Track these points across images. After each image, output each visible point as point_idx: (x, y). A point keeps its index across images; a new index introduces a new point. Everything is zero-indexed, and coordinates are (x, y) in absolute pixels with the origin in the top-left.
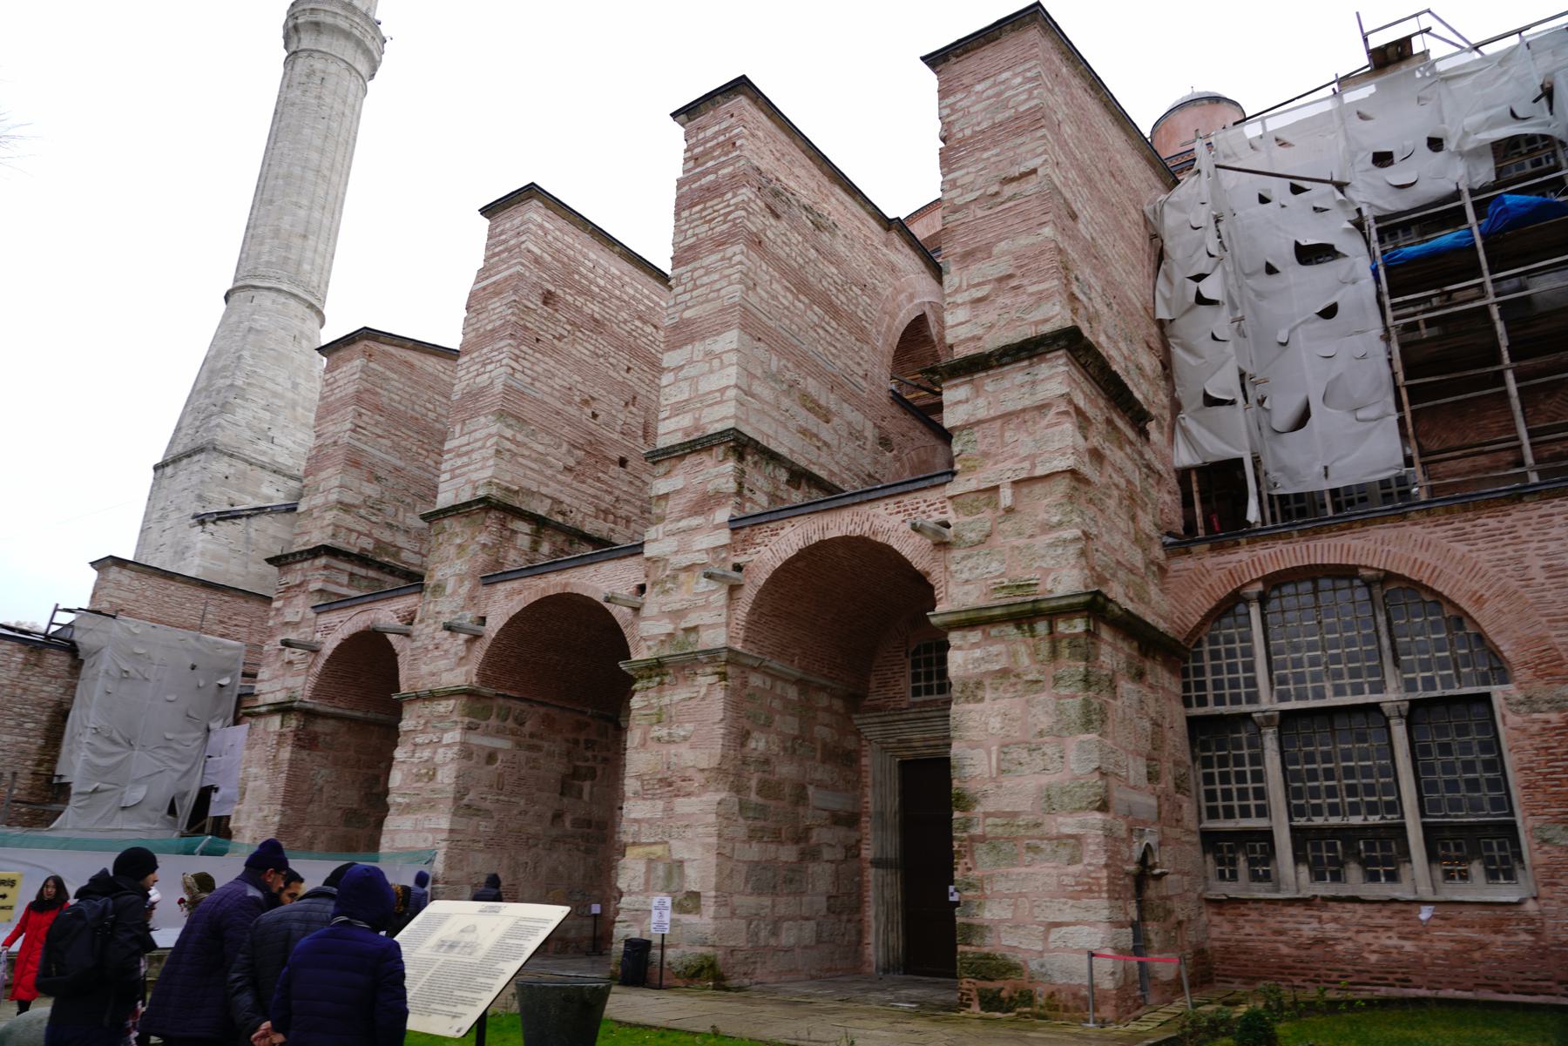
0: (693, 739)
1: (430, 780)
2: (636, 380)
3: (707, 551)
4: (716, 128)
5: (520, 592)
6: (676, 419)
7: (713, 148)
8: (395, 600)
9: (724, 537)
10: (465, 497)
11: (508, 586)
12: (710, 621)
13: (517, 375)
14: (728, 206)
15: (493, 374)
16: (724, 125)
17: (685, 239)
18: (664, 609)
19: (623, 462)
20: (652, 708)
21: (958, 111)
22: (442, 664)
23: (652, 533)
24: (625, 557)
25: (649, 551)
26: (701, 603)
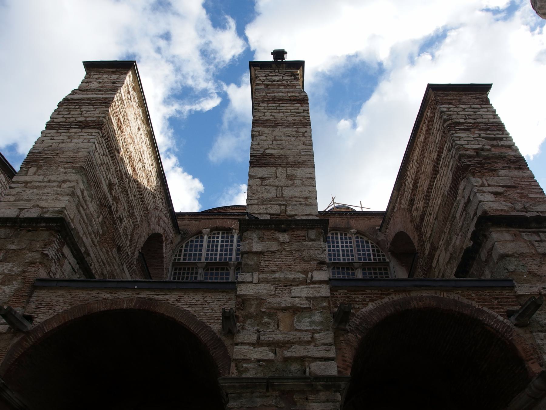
2: (135, 204)
3: (308, 298)
4: (281, 78)
6: (265, 207)
7: (279, 85)
9: (325, 291)
10: (34, 213)
12: (318, 355)
13: (97, 154)
14: (298, 109)
15: (78, 145)
16: (285, 78)
17: (264, 116)
18: (262, 338)
19: (119, 249)
21: (450, 111)
23: (246, 277)
25: (242, 290)
26: (308, 337)
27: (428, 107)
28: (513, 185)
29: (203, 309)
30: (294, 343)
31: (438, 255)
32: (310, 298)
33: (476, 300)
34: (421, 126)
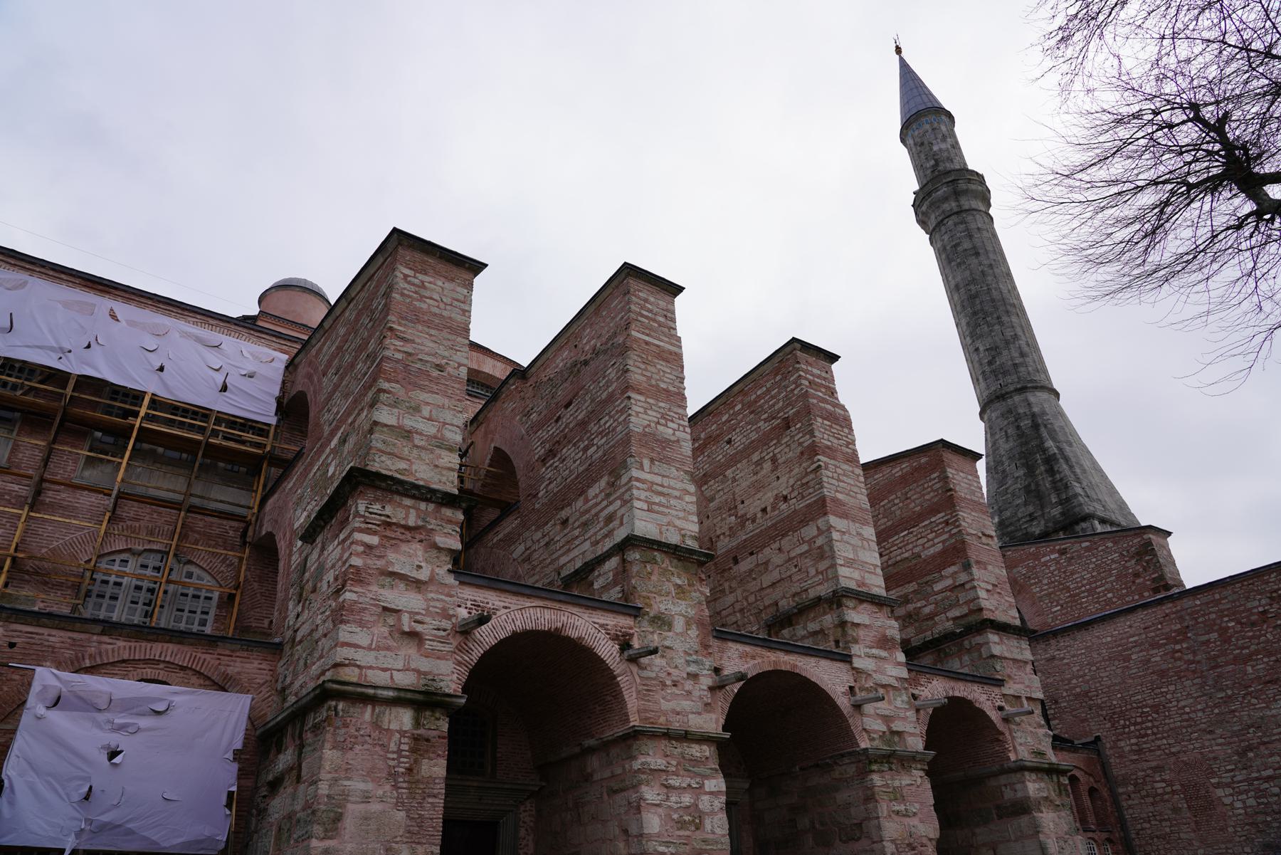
0: (920, 815)
1: (697, 829)
5: (753, 658)
8: (600, 613)
11: (741, 647)
18: (878, 711)
20: (889, 787)
22: (686, 704)
24: (836, 660)
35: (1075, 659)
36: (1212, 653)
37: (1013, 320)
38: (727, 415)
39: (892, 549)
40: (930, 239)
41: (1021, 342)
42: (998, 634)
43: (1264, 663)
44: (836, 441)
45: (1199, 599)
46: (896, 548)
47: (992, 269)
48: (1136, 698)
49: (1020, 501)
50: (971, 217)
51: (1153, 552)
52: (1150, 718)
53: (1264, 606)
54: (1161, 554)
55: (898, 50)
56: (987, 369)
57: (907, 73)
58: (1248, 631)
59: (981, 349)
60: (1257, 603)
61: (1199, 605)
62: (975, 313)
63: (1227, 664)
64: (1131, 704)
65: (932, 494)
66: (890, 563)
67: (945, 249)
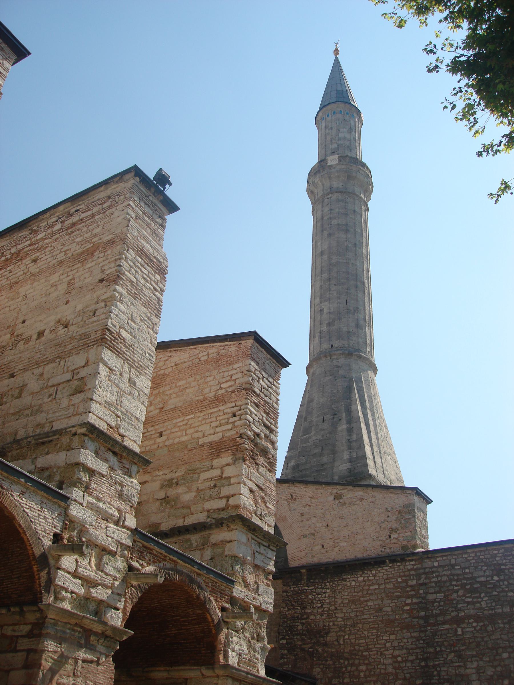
18: (80, 570)
27: (235, 342)
28: (263, 487)
29: (39, 517)
30: (99, 584)
31: (146, 479)
32: (119, 542)
33: (210, 589)
34: (212, 344)
35: (319, 596)
36: (434, 611)
37: (359, 295)
38: (44, 233)
39: (173, 430)
40: (313, 208)
41: (360, 315)
42: (247, 534)
43: (472, 627)
44: (143, 281)
45: (438, 561)
46: (177, 429)
47: (355, 247)
48: (360, 641)
49: (317, 451)
50: (352, 200)
51: (412, 512)
52: (366, 662)
53: (487, 577)
54: (419, 515)
55: (336, 51)
56: (325, 328)
57: (337, 68)
58: (469, 597)
59: (326, 311)
60: (482, 573)
61: (436, 567)
62: (329, 279)
63: (444, 623)
64: (354, 646)
65: (229, 383)
66: (166, 444)
67: (322, 218)
